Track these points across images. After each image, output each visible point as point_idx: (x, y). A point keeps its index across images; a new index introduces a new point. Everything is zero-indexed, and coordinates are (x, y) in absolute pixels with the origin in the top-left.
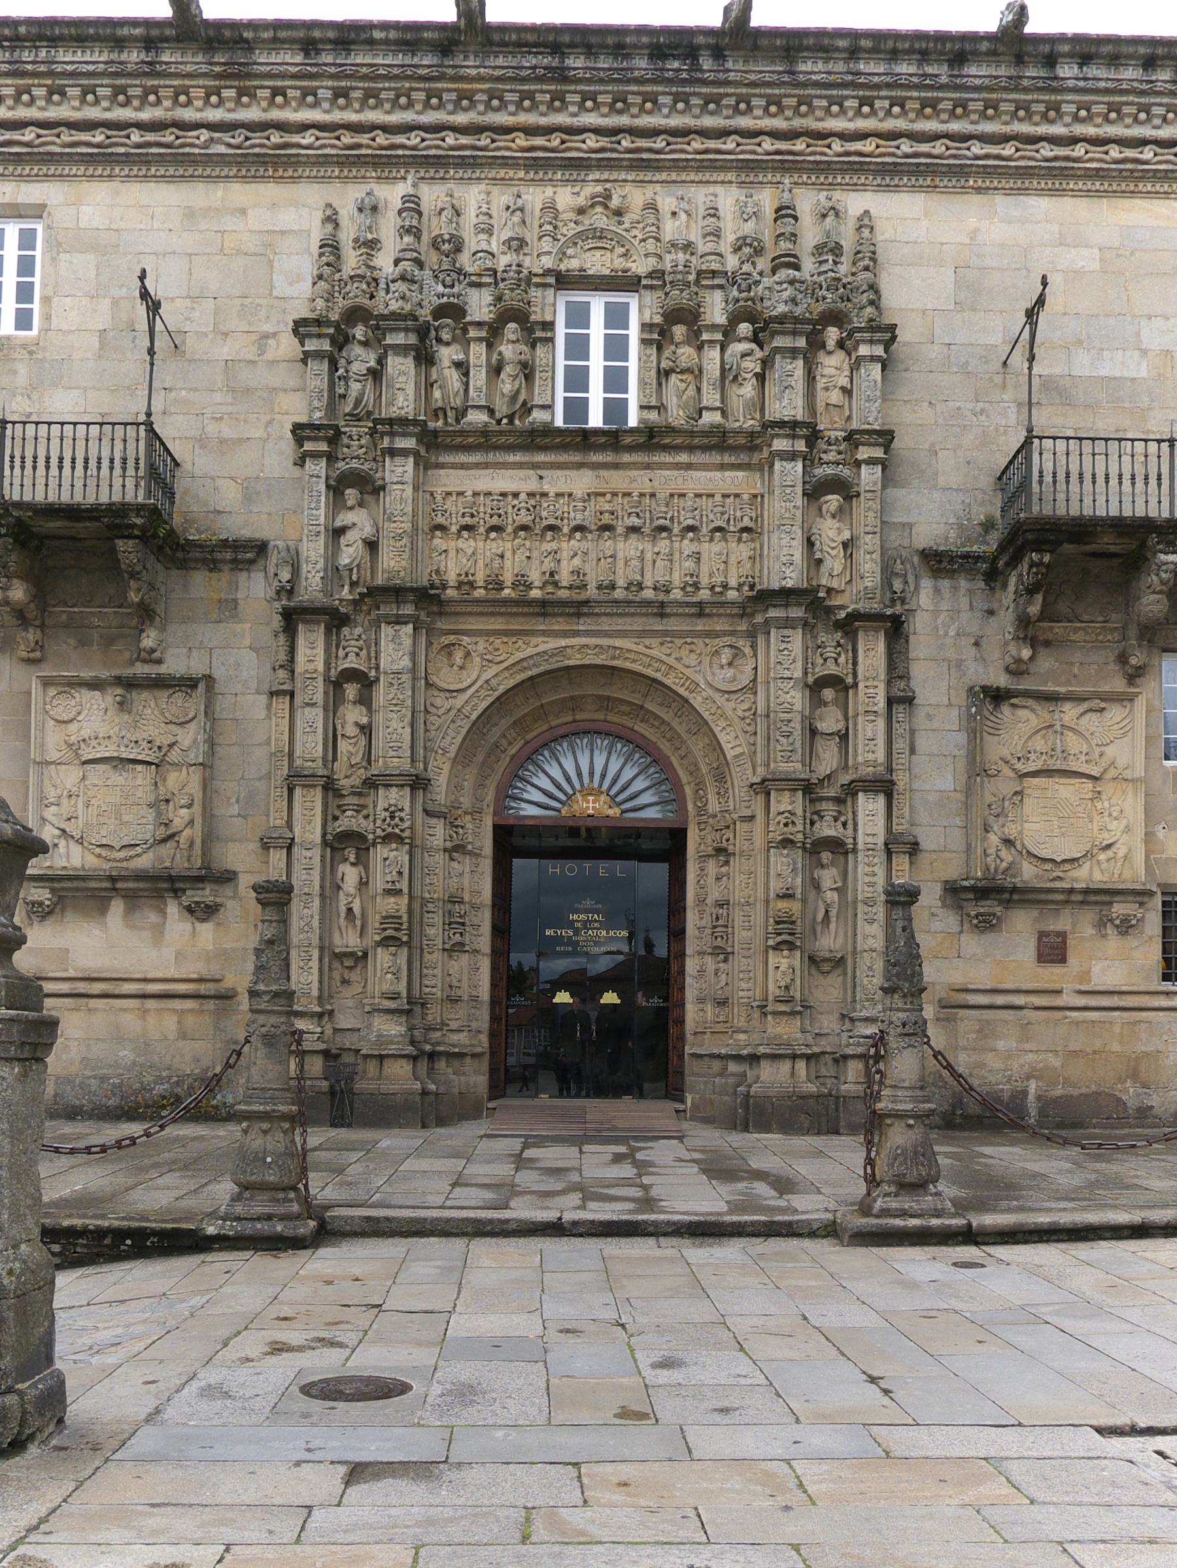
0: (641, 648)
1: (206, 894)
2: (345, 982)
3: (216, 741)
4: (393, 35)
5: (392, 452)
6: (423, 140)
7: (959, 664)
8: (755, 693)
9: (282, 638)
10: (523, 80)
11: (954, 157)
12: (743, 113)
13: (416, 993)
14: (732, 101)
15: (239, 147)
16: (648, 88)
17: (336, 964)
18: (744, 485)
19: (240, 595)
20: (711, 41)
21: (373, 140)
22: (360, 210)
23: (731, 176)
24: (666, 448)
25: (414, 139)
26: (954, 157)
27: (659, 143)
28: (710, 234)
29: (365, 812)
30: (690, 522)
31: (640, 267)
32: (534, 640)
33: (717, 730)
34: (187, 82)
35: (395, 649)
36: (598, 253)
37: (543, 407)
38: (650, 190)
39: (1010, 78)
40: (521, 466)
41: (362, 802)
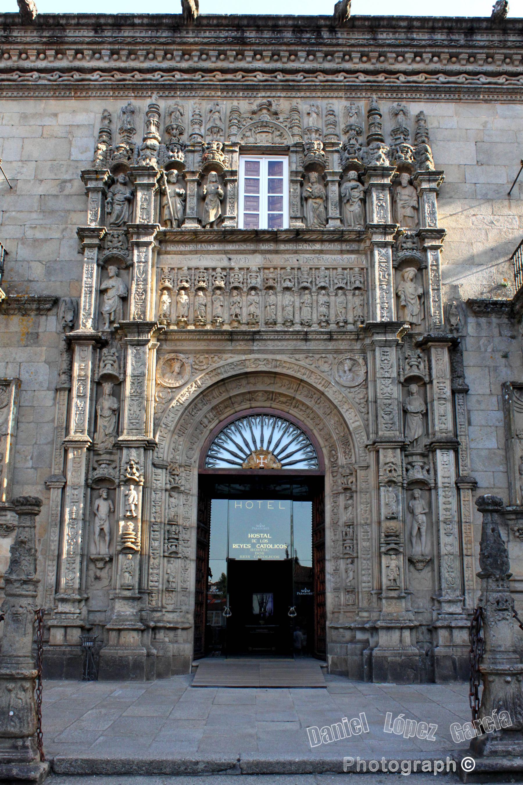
0: (293, 360)
2: (97, 578)
3: (20, 420)
4: (145, 21)
5: (138, 245)
6: (162, 77)
7: (496, 368)
8: (367, 388)
9: (65, 356)
10: (221, 44)
11: (471, 83)
12: (348, 61)
13: (145, 586)
14: (341, 54)
15: (55, 81)
16: (293, 48)
17: (92, 566)
18: (355, 263)
19: (41, 330)
20: (328, 23)
21: (133, 76)
22: (124, 113)
23: (341, 94)
24: (306, 241)
25: (157, 76)
26: (471, 83)
27: (299, 77)
28: (330, 124)
29: (113, 465)
30: (323, 284)
31: (290, 141)
32: (225, 356)
33: (343, 411)
34: (27, 47)
36: (264, 135)
37: (232, 218)
38: (294, 102)
39: (500, 41)
40: (217, 252)
41: (112, 457)
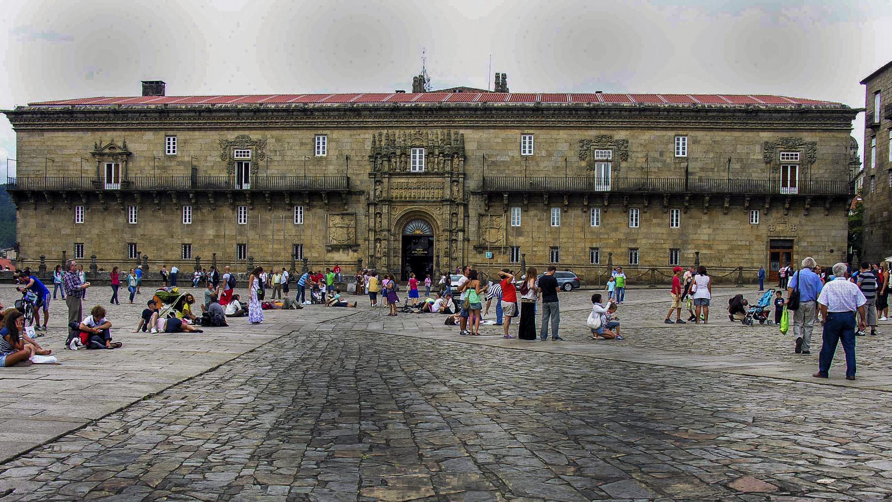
1: (355, 248)
31: (425, 144)
35: (385, 209)
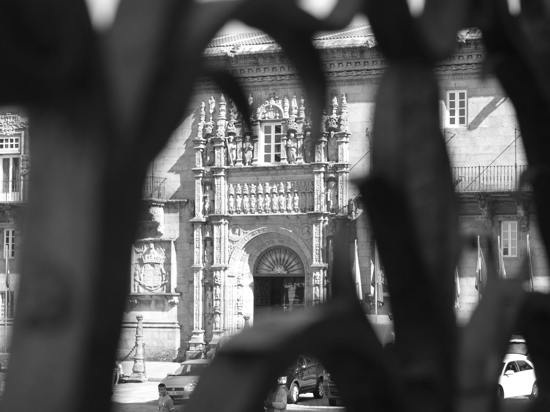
40: (252, 175)
